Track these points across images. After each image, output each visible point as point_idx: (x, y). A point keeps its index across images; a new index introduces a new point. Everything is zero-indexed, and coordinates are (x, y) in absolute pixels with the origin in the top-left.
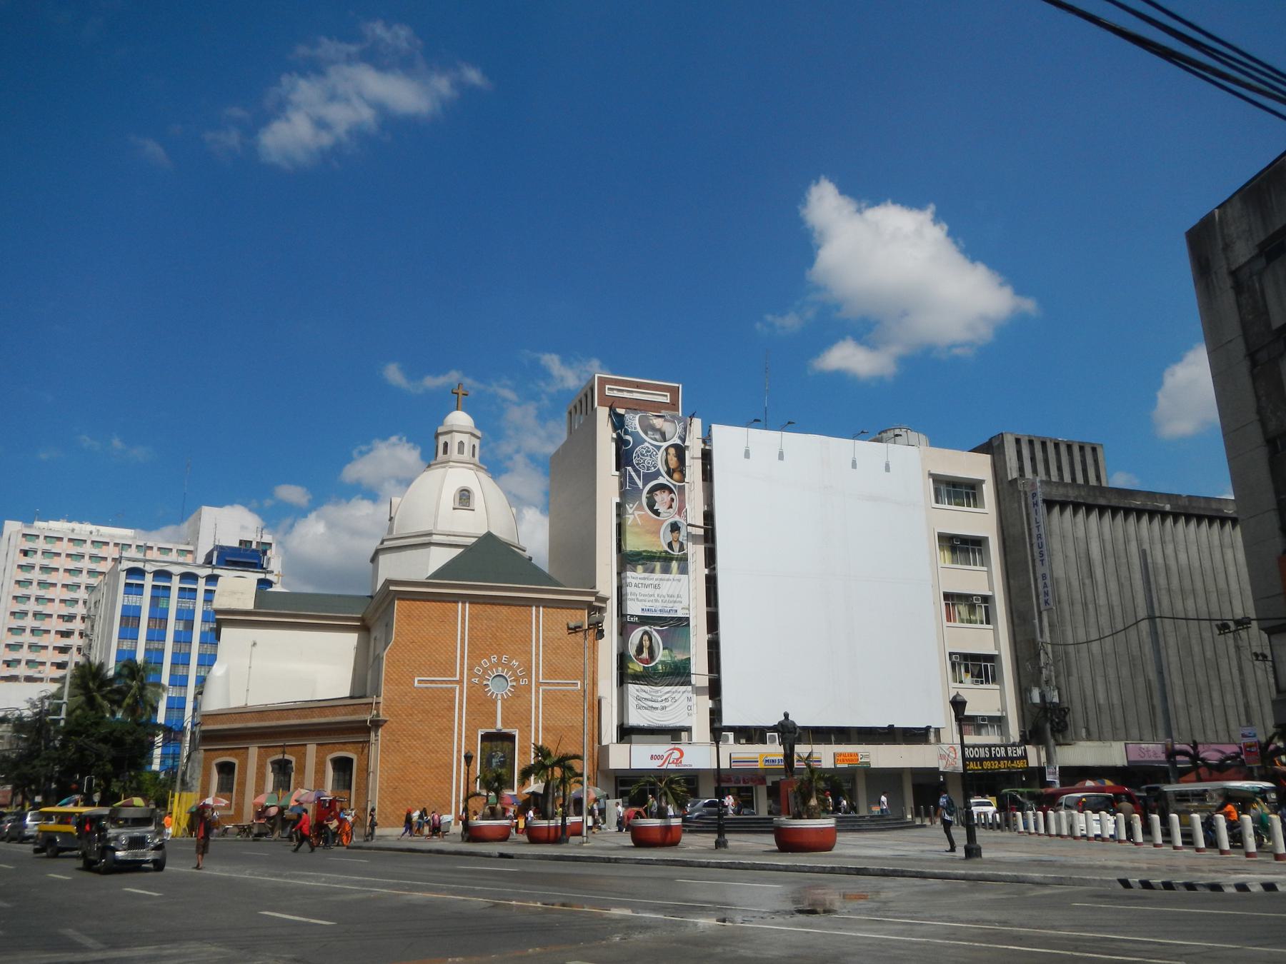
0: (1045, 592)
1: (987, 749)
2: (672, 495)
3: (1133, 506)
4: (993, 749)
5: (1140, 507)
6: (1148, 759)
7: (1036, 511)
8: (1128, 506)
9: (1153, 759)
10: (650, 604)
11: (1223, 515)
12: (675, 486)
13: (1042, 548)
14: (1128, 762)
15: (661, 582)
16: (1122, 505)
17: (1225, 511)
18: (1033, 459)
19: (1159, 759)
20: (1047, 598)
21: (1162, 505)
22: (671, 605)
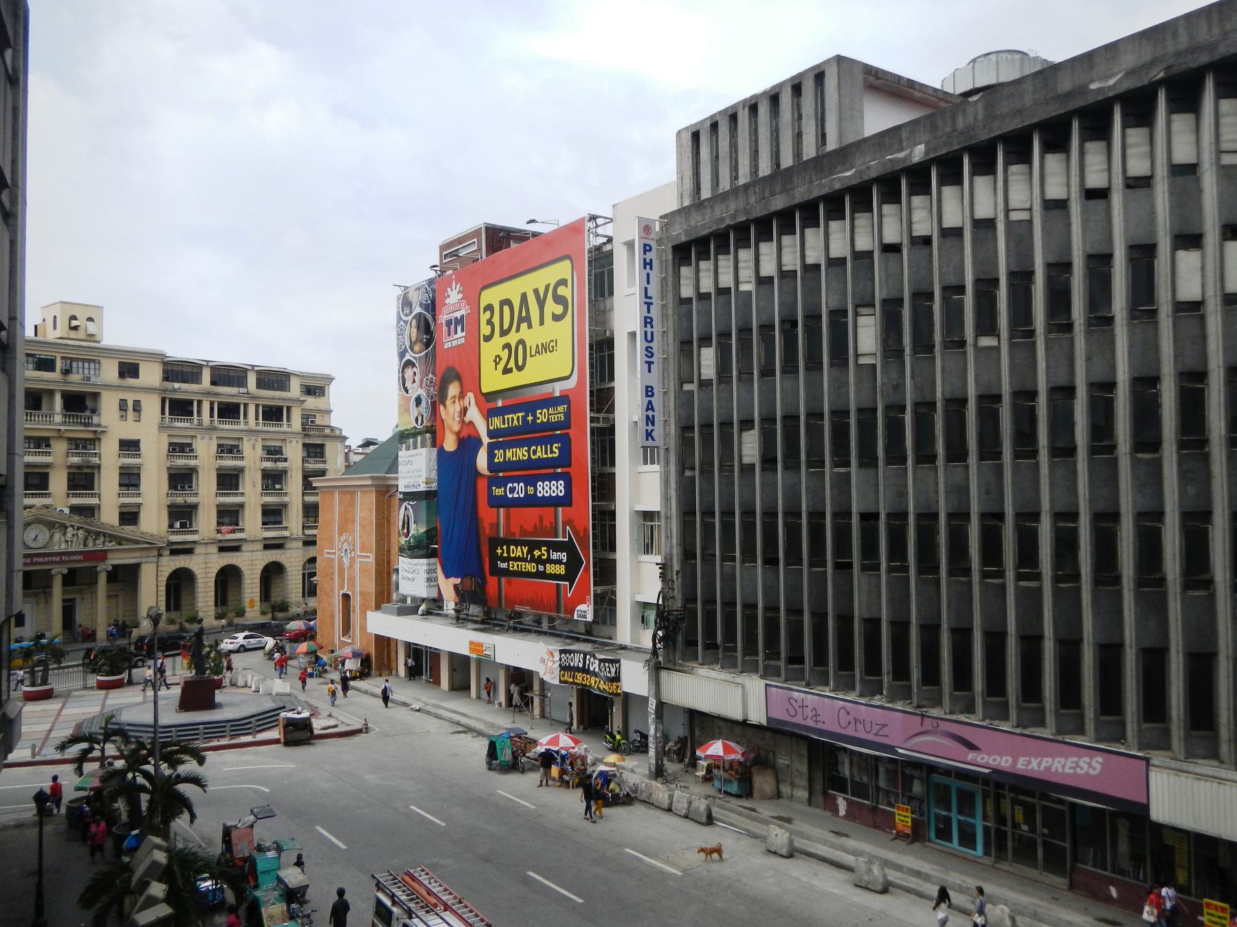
0: (647, 417)
1: (582, 655)
2: (415, 369)
3: (837, 186)
4: (588, 657)
5: (854, 182)
6: (802, 722)
7: (648, 275)
8: (825, 191)
9: (810, 723)
10: (413, 480)
11: (1091, 99)
12: (415, 358)
13: (652, 341)
14: (769, 719)
15: (412, 458)
16: (815, 194)
17: (1093, 86)
18: (716, 158)
19: (820, 726)
20: (650, 428)
21: (901, 155)
22: (413, 480)
